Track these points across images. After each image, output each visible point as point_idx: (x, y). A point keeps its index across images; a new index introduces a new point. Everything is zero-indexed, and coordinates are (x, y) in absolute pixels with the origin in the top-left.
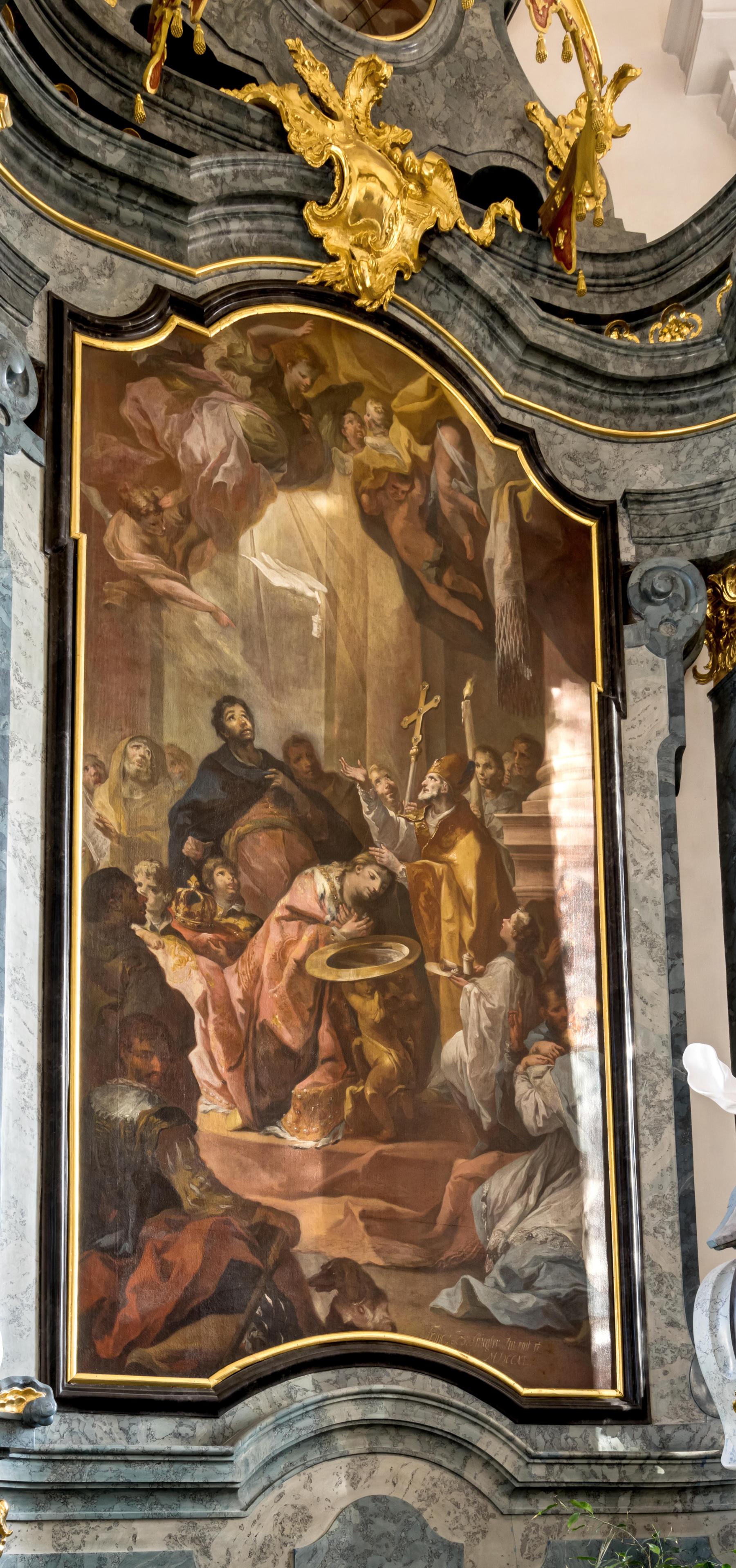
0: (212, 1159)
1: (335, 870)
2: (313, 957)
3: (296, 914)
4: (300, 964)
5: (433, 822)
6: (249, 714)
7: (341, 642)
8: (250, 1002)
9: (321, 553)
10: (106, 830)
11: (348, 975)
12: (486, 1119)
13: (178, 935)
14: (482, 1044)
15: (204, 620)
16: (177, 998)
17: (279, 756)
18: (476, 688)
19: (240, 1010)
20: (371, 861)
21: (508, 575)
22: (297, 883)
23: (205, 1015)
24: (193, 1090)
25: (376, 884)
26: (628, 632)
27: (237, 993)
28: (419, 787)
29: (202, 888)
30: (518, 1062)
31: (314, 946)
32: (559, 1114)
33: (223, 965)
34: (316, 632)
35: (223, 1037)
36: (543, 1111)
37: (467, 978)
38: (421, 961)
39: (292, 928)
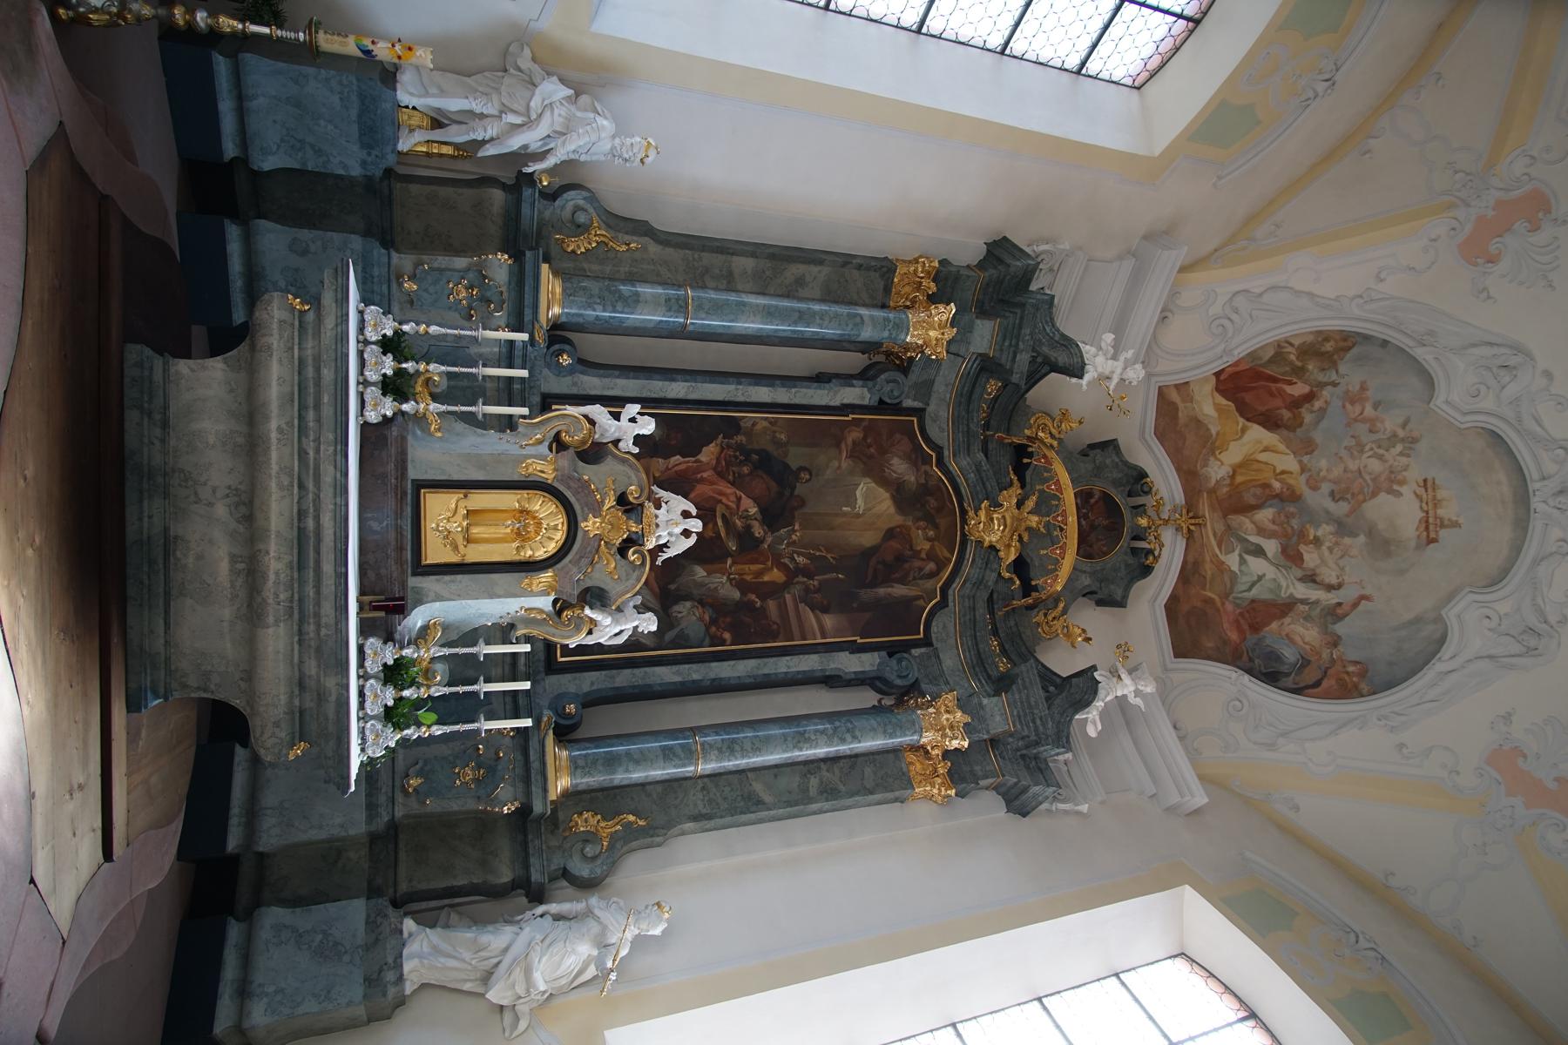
1: (759, 516)
2: (724, 507)
3: (739, 499)
4: (720, 501)
5: (786, 561)
6: (807, 481)
7: (844, 519)
8: (702, 481)
9: (874, 511)
10: (753, 425)
11: (720, 523)
12: (672, 587)
13: (722, 452)
14: (702, 585)
15: (836, 464)
16: (700, 452)
17: (796, 493)
18: (841, 580)
19: (699, 476)
20: (766, 533)
21: (889, 594)
22: (750, 501)
23: (695, 462)
24: (667, 457)
25: (757, 535)
26: (884, 654)
27: (705, 475)
28: (799, 554)
29: (741, 461)
30: (699, 603)
31: (727, 507)
32: (679, 624)
33: (715, 469)
34: (844, 509)
35: (688, 468)
36: (680, 615)
37: (728, 578)
38: (732, 556)
39: (733, 498)
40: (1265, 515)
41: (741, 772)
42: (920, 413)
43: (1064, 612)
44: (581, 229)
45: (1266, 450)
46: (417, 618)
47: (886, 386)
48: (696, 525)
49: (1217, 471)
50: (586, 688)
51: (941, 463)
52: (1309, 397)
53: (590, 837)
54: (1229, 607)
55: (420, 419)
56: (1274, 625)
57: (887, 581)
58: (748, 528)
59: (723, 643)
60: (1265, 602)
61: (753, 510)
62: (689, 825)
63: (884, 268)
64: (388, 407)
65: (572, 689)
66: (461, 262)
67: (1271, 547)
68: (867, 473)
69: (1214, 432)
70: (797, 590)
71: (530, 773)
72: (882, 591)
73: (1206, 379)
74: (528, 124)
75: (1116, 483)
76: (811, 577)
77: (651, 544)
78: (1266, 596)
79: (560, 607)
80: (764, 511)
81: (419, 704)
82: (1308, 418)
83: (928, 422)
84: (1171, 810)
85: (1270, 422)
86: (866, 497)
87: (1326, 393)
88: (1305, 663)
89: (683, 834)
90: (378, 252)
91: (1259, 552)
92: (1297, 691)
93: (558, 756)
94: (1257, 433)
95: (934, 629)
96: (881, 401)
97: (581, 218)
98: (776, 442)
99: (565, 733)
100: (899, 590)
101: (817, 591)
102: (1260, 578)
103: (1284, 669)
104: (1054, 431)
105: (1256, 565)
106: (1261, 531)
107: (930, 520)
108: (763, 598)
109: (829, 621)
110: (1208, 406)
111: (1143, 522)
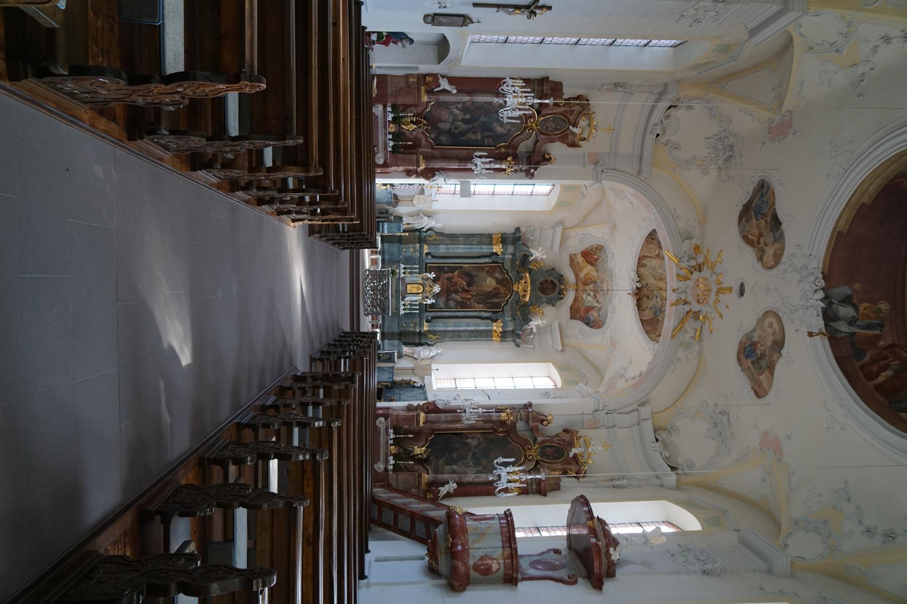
0: (443, 275)
3: (462, 282)
40: (591, 286)
41: (459, 331)
42: (503, 263)
43: (538, 306)
44: (431, 237)
45: (591, 271)
46: (406, 299)
47: (494, 258)
48: (440, 289)
49: (582, 275)
50: (432, 315)
51: (507, 274)
52: (598, 259)
53: (431, 338)
54: (583, 307)
55: (407, 276)
56: (590, 312)
57: (493, 298)
58: (464, 287)
59: (458, 309)
60: (590, 307)
61: (465, 284)
62: (448, 339)
63: (490, 236)
64: (404, 275)
65: (430, 315)
66: (412, 246)
67: (592, 293)
68: (490, 276)
69: (581, 265)
70: (474, 299)
71: (421, 325)
72: (492, 300)
73: (579, 253)
74: (422, 225)
75: (555, 278)
76: (477, 297)
77: (434, 291)
78: (590, 305)
79: (422, 299)
80: (467, 284)
81: (406, 308)
82: (598, 264)
83: (505, 265)
84: (556, 350)
85: (592, 264)
86: (489, 282)
87: (600, 258)
88: (594, 320)
89: (448, 341)
90: (400, 245)
91: (589, 295)
92: (591, 327)
93: (426, 324)
94: (589, 266)
95: (505, 308)
96: (493, 261)
97: (431, 235)
98: (470, 271)
99: (427, 321)
100: (496, 300)
101: (478, 299)
102: (589, 301)
103: (590, 322)
104: (538, 267)
105: (589, 298)
106: (590, 290)
107: (504, 286)
108: (467, 300)
109: (480, 306)
110: (580, 259)
111: (562, 287)
